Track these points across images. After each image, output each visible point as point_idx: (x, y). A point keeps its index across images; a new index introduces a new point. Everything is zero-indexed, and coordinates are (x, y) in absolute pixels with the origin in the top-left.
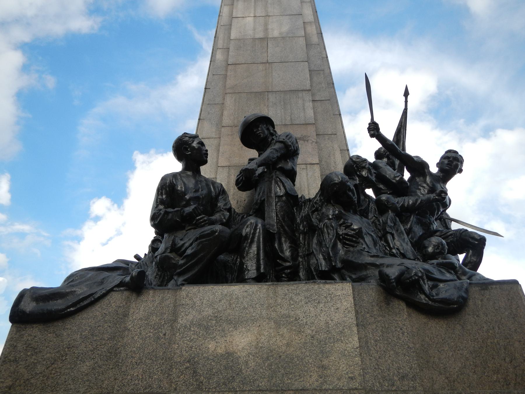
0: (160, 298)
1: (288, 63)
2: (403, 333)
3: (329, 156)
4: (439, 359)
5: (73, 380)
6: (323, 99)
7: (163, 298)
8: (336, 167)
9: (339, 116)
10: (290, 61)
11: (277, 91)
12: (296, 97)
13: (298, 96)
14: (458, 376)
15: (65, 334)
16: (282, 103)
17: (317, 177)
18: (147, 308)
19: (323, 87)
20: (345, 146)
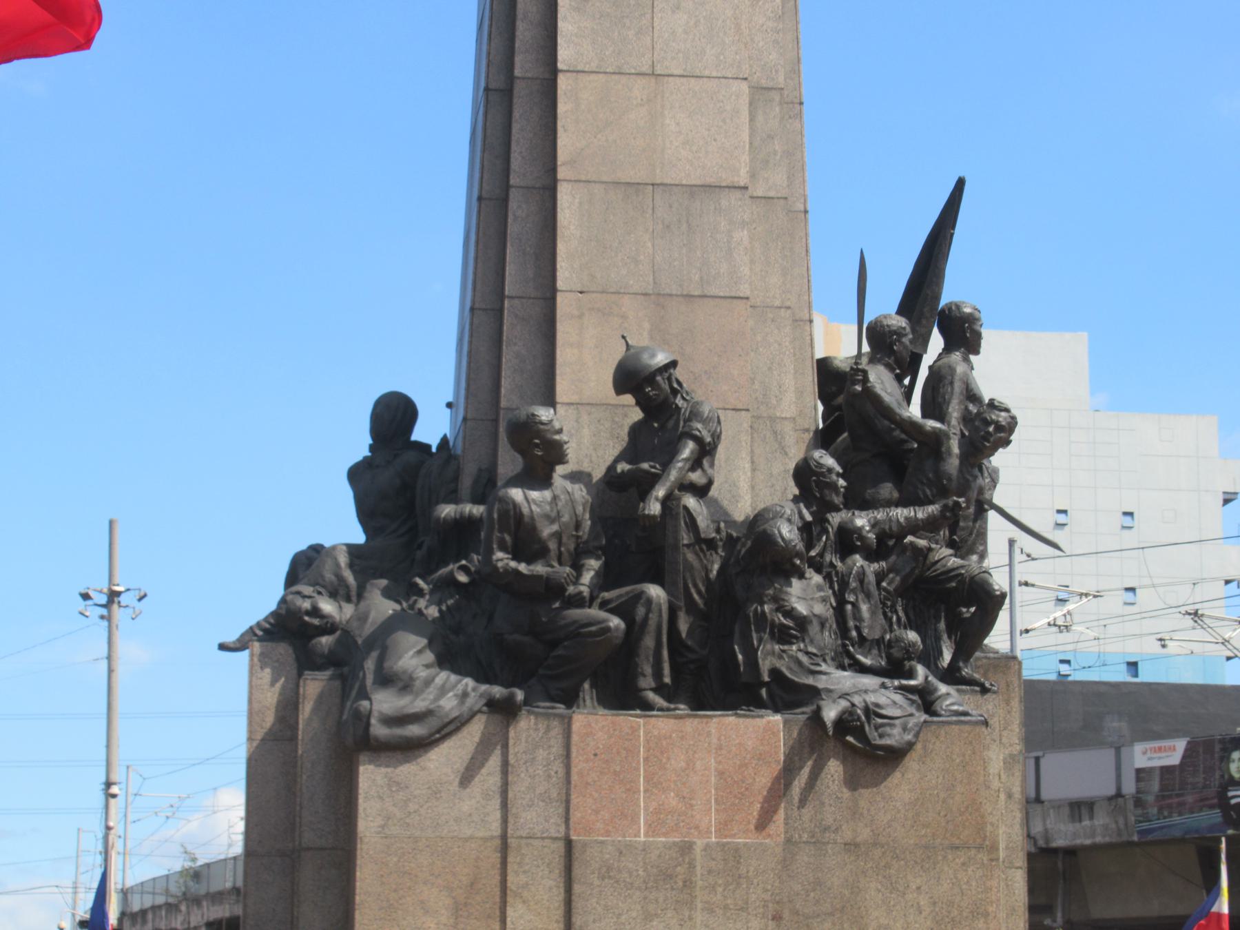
0: (545, 726)
1: (701, 81)
2: (833, 781)
3: (770, 369)
4: (869, 810)
5: (455, 820)
6: (772, 194)
7: (548, 726)
8: (781, 399)
9: (803, 215)
10: (707, 73)
11: (673, 182)
12: (715, 209)
13: (720, 204)
14: (884, 829)
15: (432, 766)
16: (684, 227)
17: (744, 444)
18: (530, 739)
19: (775, 153)
20: (806, 311)
